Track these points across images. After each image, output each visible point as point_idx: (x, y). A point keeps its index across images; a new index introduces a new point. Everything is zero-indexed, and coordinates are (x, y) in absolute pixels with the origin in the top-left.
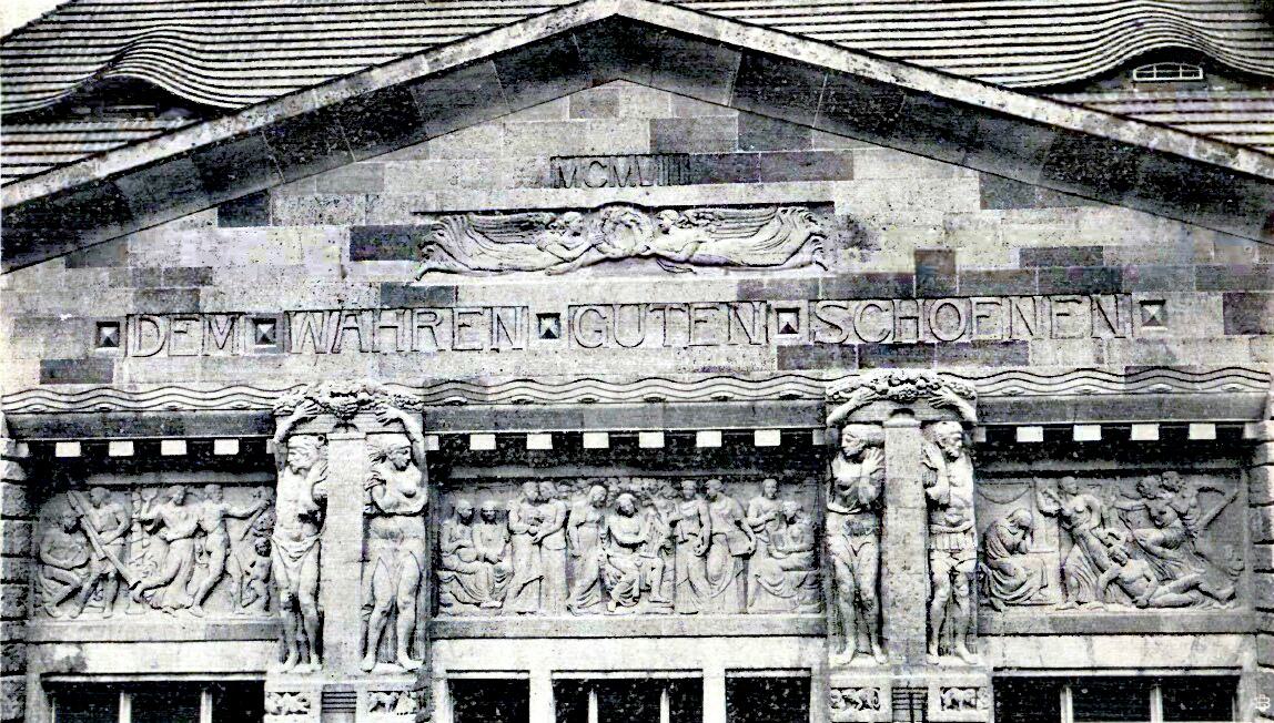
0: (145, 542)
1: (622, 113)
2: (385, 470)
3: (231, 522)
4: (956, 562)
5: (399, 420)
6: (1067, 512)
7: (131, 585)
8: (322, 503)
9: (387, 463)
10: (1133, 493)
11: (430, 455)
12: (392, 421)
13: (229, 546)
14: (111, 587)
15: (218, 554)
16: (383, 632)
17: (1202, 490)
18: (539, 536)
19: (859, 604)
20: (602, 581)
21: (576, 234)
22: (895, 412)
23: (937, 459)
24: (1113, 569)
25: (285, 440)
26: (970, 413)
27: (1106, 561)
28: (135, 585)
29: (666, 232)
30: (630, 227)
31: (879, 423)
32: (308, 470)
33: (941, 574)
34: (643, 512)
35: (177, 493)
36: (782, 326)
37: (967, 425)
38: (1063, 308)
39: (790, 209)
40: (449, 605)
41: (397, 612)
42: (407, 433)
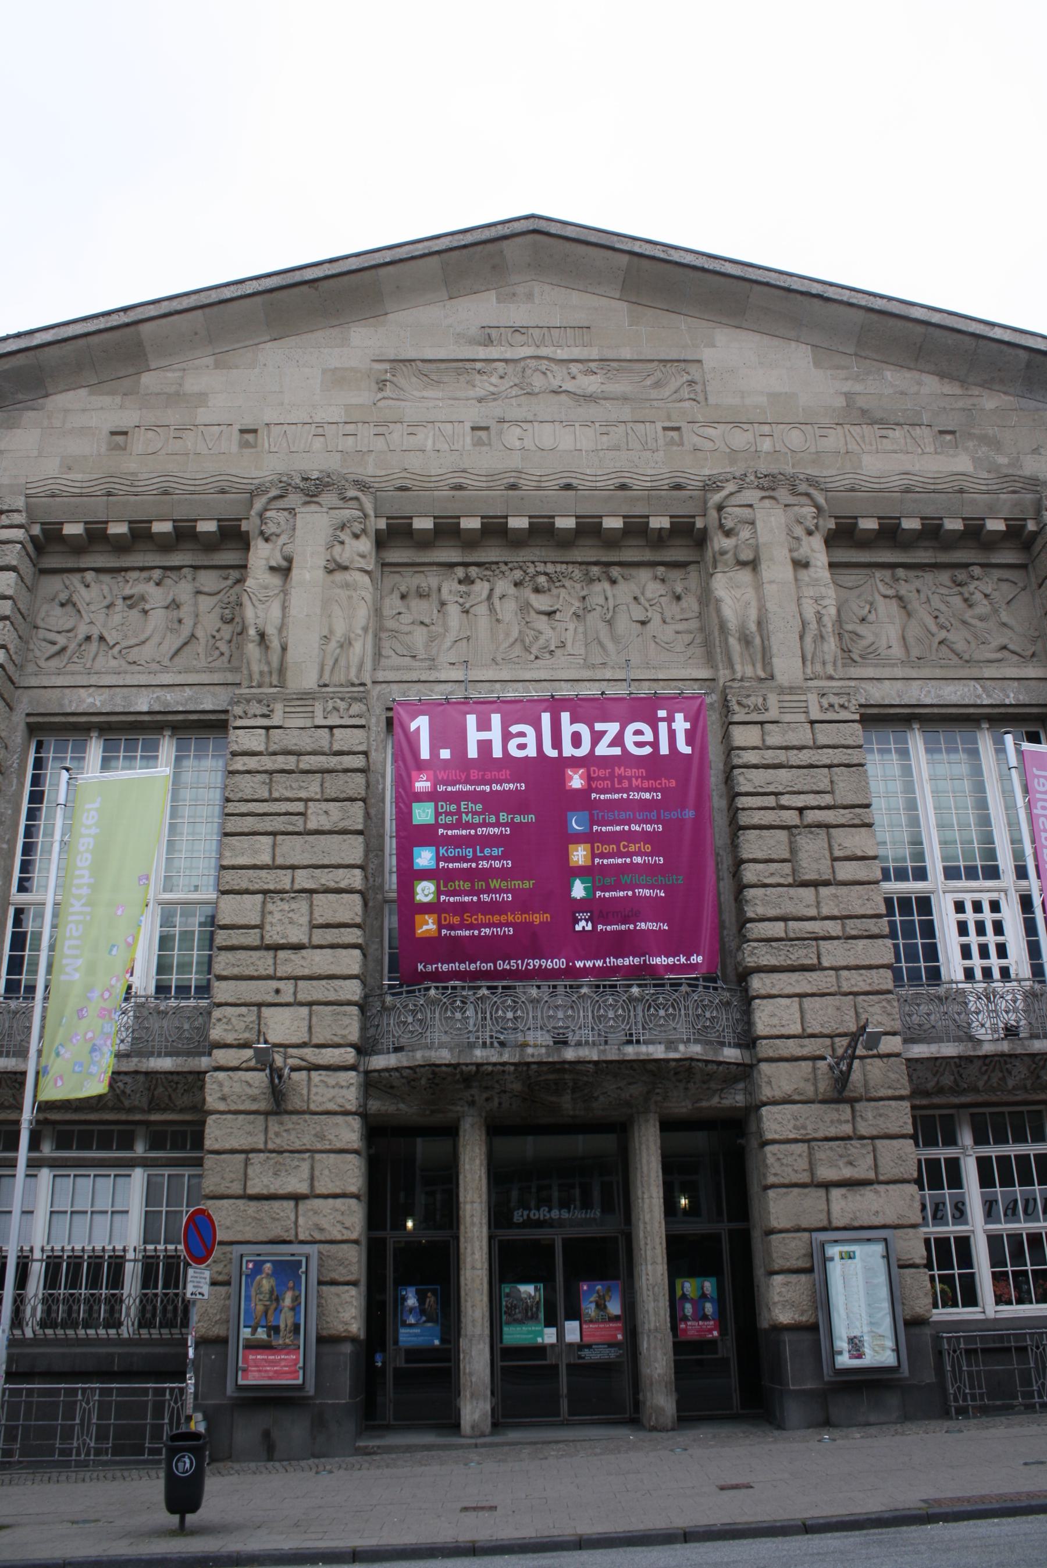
0: (125, 614)
1: (537, 301)
2: (345, 536)
3: (201, 598)
4: (820, 608)
5: (357, 499)
6: (903, 592)
7: (111, 644)
8: (289, 560)
9: (348, 531)
10: (949, 584)
12: (351, 499)
13: (197, 616)
14: (94, 645)
15: (188, 622)
16: (336, 660)
17: (999, 580)
18: (467, 605)
19: (746, 640)
20: (523, 641)
21: (501, 377)
22: (763, 498)
23: (799, 531)
24: (943, 634)
25: (261, 515)
26: (821, 499)
27: (934, 628)
28: (114, 645)
29: (574, 378)
31: (751, 506)
32: (278, 536)
33: (810, 614)
34: (555, 591)
35: (157, 574)
36: (668, 439)
38: (884, 432)
39: (669, 365)
40: (388, 657)
41: (350, 643)
42: (362, 510)
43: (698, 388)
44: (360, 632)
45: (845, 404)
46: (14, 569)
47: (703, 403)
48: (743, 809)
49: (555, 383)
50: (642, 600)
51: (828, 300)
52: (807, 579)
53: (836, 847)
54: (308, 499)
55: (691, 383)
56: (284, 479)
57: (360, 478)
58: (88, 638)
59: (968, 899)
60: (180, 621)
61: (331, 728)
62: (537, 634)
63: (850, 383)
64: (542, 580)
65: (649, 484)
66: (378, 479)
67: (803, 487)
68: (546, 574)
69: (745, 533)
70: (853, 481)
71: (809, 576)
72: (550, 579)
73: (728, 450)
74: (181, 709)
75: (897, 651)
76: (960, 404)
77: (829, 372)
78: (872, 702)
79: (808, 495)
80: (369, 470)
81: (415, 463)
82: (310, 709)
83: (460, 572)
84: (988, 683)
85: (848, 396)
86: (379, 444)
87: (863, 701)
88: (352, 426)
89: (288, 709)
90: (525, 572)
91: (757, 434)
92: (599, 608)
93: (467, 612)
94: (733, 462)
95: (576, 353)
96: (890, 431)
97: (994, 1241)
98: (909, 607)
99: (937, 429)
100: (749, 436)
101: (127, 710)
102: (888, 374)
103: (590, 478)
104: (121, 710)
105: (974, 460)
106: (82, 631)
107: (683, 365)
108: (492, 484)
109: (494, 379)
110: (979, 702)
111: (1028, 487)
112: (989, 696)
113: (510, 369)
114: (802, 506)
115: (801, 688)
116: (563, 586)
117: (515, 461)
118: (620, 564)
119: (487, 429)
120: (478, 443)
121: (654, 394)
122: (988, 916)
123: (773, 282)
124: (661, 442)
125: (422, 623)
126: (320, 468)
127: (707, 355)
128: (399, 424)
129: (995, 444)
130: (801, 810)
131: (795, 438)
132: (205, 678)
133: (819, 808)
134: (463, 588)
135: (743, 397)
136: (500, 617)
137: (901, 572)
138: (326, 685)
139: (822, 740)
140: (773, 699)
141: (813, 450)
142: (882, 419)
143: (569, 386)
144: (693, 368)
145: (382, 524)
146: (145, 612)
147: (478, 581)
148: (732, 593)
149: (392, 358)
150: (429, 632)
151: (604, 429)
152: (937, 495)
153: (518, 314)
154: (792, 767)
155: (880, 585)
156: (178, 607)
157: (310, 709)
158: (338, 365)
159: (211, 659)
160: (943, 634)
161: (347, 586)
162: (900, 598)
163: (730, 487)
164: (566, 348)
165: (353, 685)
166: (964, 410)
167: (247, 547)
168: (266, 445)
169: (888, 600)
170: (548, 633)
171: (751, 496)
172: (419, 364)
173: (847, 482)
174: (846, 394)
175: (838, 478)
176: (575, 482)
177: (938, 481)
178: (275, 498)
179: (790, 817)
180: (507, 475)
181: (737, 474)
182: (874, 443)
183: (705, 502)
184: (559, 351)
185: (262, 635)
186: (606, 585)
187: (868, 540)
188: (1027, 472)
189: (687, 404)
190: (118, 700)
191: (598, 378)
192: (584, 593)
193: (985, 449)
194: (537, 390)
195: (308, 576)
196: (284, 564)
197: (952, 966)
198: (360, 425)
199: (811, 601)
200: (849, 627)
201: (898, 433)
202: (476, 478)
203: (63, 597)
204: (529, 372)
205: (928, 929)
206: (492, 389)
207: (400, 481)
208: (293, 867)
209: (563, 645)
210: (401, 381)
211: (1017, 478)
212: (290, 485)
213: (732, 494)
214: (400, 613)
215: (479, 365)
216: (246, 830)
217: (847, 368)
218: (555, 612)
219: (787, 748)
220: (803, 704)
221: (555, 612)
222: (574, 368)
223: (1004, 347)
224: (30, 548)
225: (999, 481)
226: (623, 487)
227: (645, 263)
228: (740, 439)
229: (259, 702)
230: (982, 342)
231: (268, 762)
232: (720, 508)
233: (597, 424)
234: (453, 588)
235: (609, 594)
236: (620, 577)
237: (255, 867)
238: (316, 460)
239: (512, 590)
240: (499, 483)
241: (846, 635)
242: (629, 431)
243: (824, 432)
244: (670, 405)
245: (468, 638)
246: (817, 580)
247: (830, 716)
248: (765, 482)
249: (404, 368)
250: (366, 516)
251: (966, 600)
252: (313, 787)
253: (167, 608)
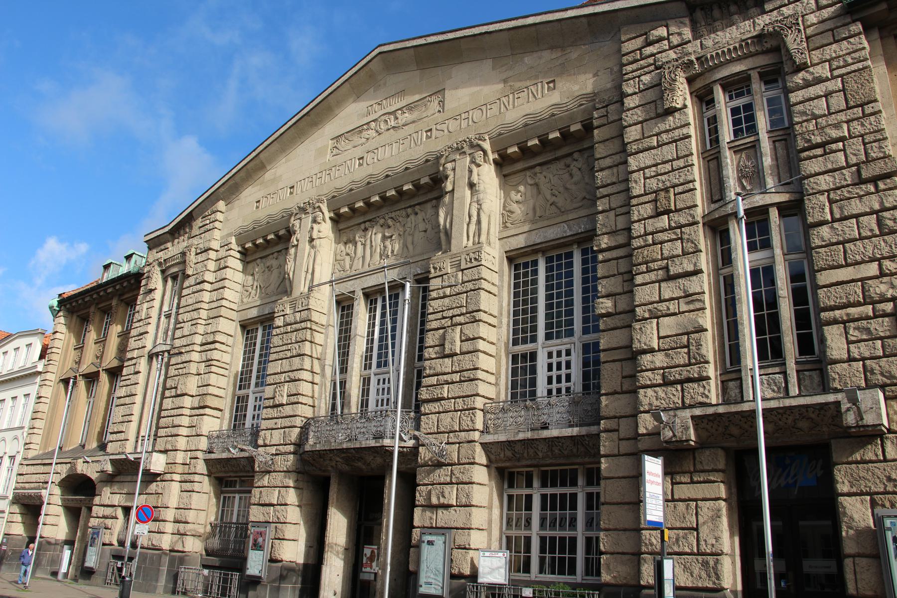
51: (491, 33)
59: (554, 350)
83: (363, 226)
87: (508, 249)
97: (543, 539)
112: (570, 230)
118: (419, 204)
122: (564, 358)
130: (451, 318)
137: (538, 169)
162: (536, 185)
176: (390, 173)
197: (542, 387)
205: (533, 370)
223: (574, 20)
227: (419, 49)
230: (563, 23)
247: (469, 265)
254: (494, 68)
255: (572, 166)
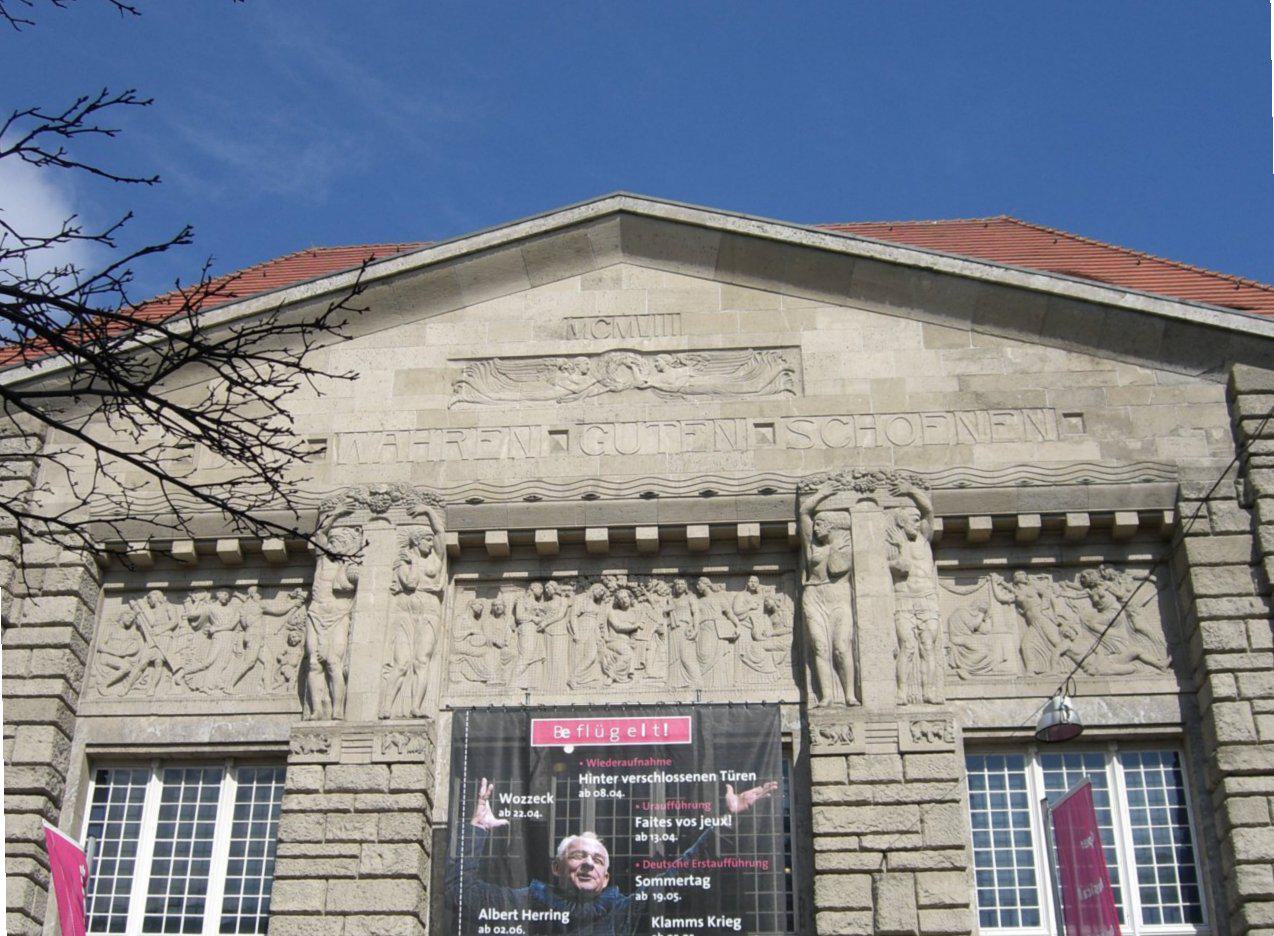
0: (191, 637)
1: (624, 287)
2: (414, 555)
4: (919, 622)
5: (426, 514)
6: (1021, 598)
8: (354, 582)
11: (449, 547)
12: (420, 514)
18: (543, 625)
21: (584, 374)
22: (860, 500)
24: (1066, 644)
26: (925, 499)
27: (1056, 638)
28: (177, 671)
29: (661, 371)
30: (630, 368)
31: (847, 510)
37: (924, 513)
38: (1000, 419)
40: (458, 682)
42: (432, 525)
43: (794, 377)
44: (424, 659)
45: (957, 389)
46: (75, 594)
47: (799, 394)
48: (822, 852)
49: (640, 378)
50: (731, 615)
51: (938, 273)
52: (906, 589)
53: (922, 894)
54: (375, 515)
55: (788, 371)
56: (352, 494)
57: (430, 491)
58: (152, 664)
60: (245, 645)
61: (389, 764)
62: (616, 655)
63: (964, 364)
64: (624, 594)
65: (737, 489)
66: (448, 492)
67: (904, 487)
68: (628, 588)
69: (839, 539)
70: (962, 476)
71: (909, 587)
72: (633, 594)
73: (825, 447)
74: (242, 739)
75: (1014, 665)
76: (1090, 382)
77: (942, 352)
78: (981, 725)
79: (911, 495)
80: (441, 482)
81: (488, 473)
82: (368, 744)
84: (1115, 699)
85: (961, 379)
86: (451, 452)
87: (970, 724)
88: (424, 434)
89: (345, 744)
90: (606, 586)
91: (858, 427)
92: (683, 626)
93: (543, 631)
94: (829, 460)
95: (665, 343)
96: (1008, 417)
98: (1029, 613)
99: (1061, 412)
100: (848, 429)
101: (187, 741)
102: (1009, 350)
103: (673, 484)
104: (181, 740)
105: (1105, 448)
106: (146, 654)
107: (779, 351)
108: (568, 494)
109: (576, 377)
110: (1104, 722)
111: (1163, 474)
112: (1115, 714)
113: (592, 363)
114: (903, 508)
115: (892, 715)
116: (647, 601)
117: (593, 468)
119: (565, 432)
120: (557, 447)
121: (746, 386)
123: (878, 256)
124: (753, 440)
125: (495, 645)
126: (389, 480)
127: (806, 339)
128: (473, 431)
129: (1127, 426)
130: (884, 852)
131: (899, 430)
132: (269, 707)
133: (905, 850)
134: (542, 604)
135: (843, 386)
136: (577, 637)
138: (385, 718)
139: (912, 774)
140: (859, 729)
141: (919, 442)
142: (999, 404)
143: (655, 380)
144: (790, 355)
145: (453, 539)
146: (210, 636)
147: (556, 597)
148: (826, 608)
149: (469, 357)
150: (502, 654)
151: (690, 429)
152: (1059, 488)
153: (604, 301)
154: (877, 804)
155: (998, 589)
156: (244, 628)
157: (368, 744)
158: (414, 367)
159: (276, 684)
160: (1066, 644)
161: (412, 608)
162: (1019, 605)
163: (824, 490)
164: (654, 339)
165: (415, 717)
166: (1093, 388)
167: (313, 566)
168: (335, 457)
169: (1006, 606)
170: (628, 653)
171: (847, 498)
172: (497, 361)
173: (956, 477)
174: (960, 378)
175: (946, 474)
176: (655, 489)
177: (1060, 472)
178: (341, 515)
179: (872, 860)
180: (585, 483)
181: (833, 475)
182: (988, 431)
183: (798, 505)
184: (645, 342)
185: (325, 664)
186: (692, 597)
187: (979, 543)
188: (1162, 457)
189: (782, 396)
190: (179, 730)
191: (687, 371)
192: (669, 608)
193: (1115, 433)
194: (620, 387)
195: (372, 600)
196: (350, 586)
198: (432, 432)
199: (908, 616)
200: (958, 640)
201: (1016, 419)
202: (552, 487)
203: (127, 619)
204: (613, 366)
206: (574, 387)
207: (472, 493)
208: (344, 914)
209: (643, 666)
210: (476, 381)
211: (1150, 465)
212: (356, 500)
213: (826, 497)
214: (472, 634)
215: (560, 361)
216: (298, 874)
217: (962, 346)
218: (635, 630)
219: (872, 783)
220: (895, 733)
221: (635, 630)
222: (662, 359)
224: (94, 570)
225: (1128, 469)
226: (708, 494)
228: (837, 434)
229: (317, 736)
231: (323, 802)
232: (813, 513)
233: (683, 423)
234: (529, 606)
235: (695, 608)
236: (708, 590)
237: (305, 913)
238: (382, 478)
239: (592, 606)
240: (575, 492)
241: (954, 648)
242: (718, 431)
243: (933, 421)
244: (763, 398)
245: (543, 660)
246: (918, 591)
247: (923, 745)
248: (863, 483)
249: (481, 367)
250: (436, 532)
251: (1095, 605)
252: (369, 827)
253: (233, 630)
254: (929, 344)
255: (1101, 590)
